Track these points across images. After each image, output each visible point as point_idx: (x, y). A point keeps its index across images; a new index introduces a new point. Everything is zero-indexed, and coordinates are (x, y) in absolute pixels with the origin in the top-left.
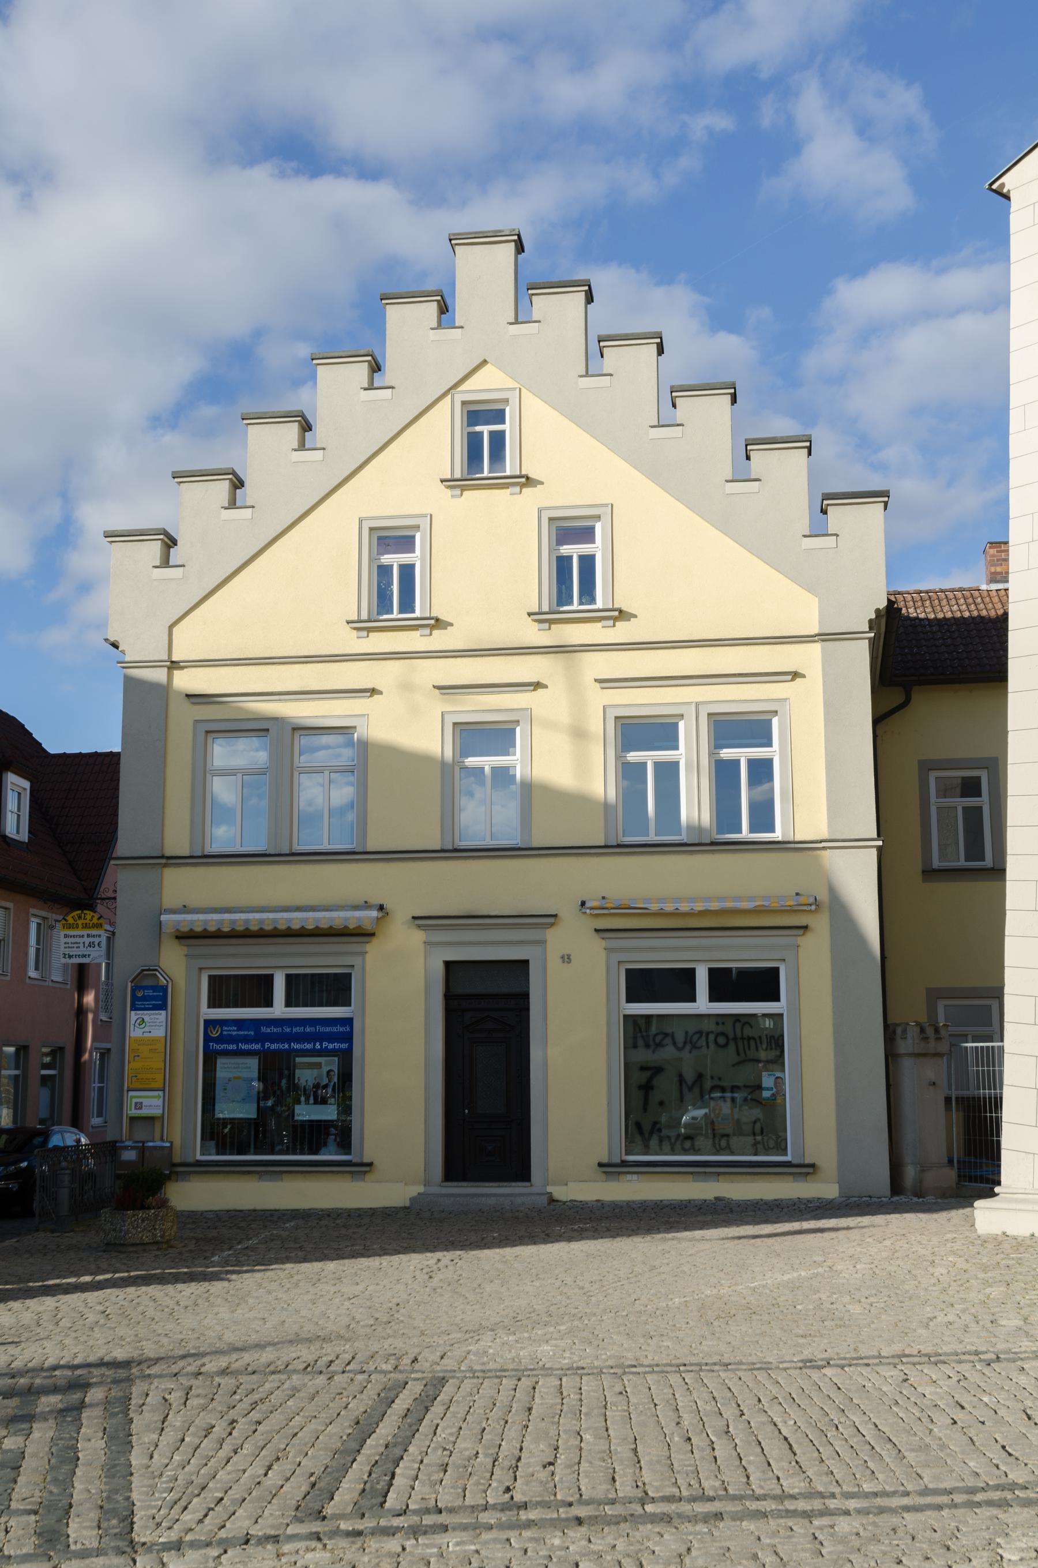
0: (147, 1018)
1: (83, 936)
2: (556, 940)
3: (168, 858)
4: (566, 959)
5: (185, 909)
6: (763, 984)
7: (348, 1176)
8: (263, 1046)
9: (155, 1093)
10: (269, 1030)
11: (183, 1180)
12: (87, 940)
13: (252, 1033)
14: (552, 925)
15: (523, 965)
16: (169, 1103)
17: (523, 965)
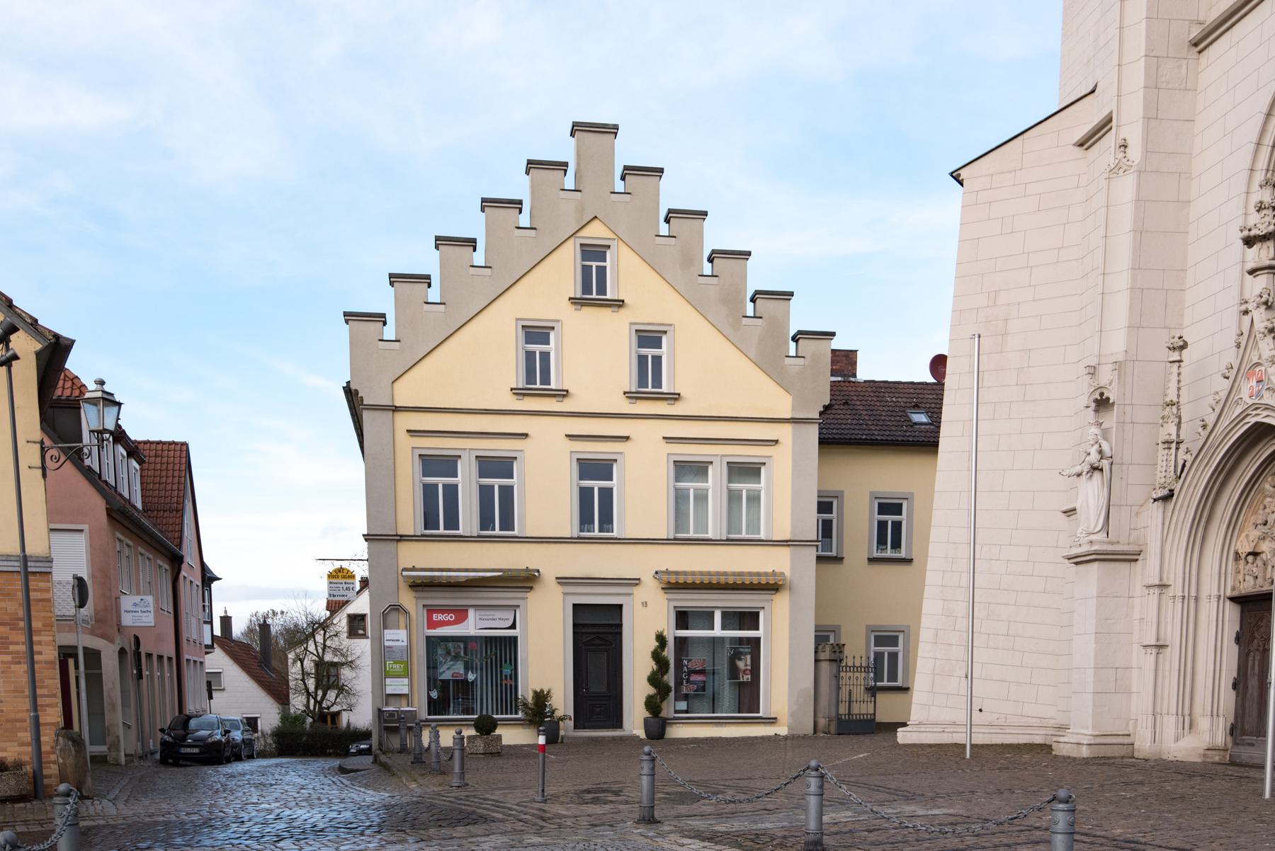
4: (645, 604)
5: (414, 569)
16: (411, 685)
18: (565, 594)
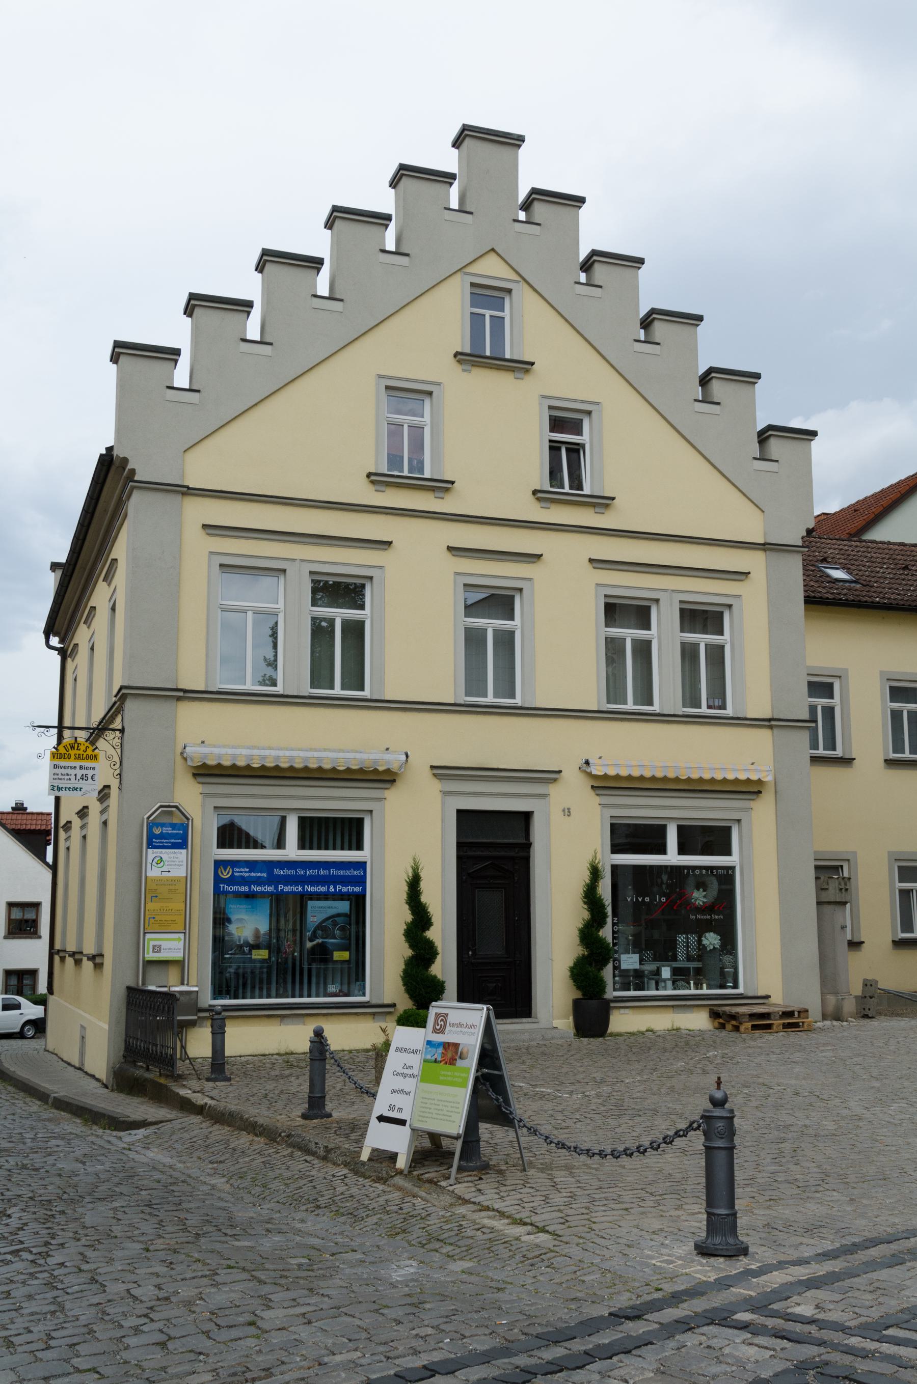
0: (165, 857)
1: (75, 768)
2: (558, 795)
3: (185, 691)
6: (715, 839)
7: (370, 1018)
8: (276, 888)
9: (176, 936)
10: (282, 873)
11: (200, 1027)
12: (80, 773)
13: (265, 875)
14: (555, 780)
15: (526, 817)
16: (187, 947)
17: (526, 817)
18: (445, 793)
